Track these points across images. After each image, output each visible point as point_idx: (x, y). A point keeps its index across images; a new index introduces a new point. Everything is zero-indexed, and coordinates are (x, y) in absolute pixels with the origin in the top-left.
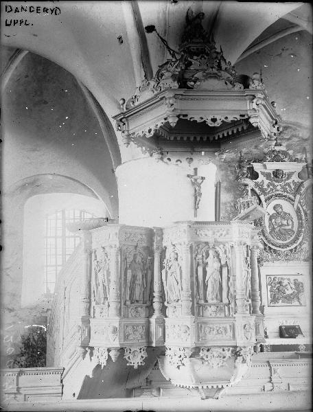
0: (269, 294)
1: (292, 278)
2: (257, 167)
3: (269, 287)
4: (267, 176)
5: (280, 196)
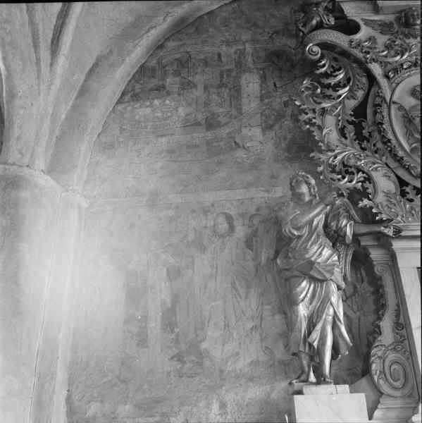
4: (385, 28)
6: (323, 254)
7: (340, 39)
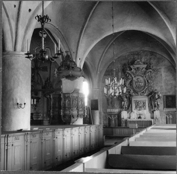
0: (135, 106)
2: (132, 67)
3: (135, 104)
4: (135, 69)
6: (125, 99)
7: (129, 72)
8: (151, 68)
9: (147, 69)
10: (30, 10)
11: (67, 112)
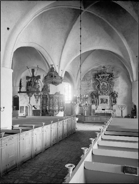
1: (105, 98)
2: (99, 75)
4: (102, 77)
5: (104, 82)
8: (112, 77)
9: (109, 77)
10: (8, 29)
11: (51, 108)
